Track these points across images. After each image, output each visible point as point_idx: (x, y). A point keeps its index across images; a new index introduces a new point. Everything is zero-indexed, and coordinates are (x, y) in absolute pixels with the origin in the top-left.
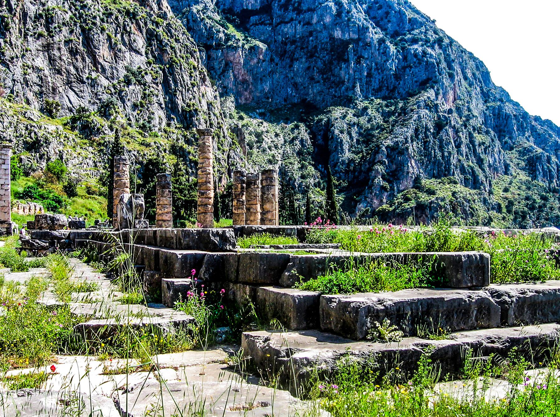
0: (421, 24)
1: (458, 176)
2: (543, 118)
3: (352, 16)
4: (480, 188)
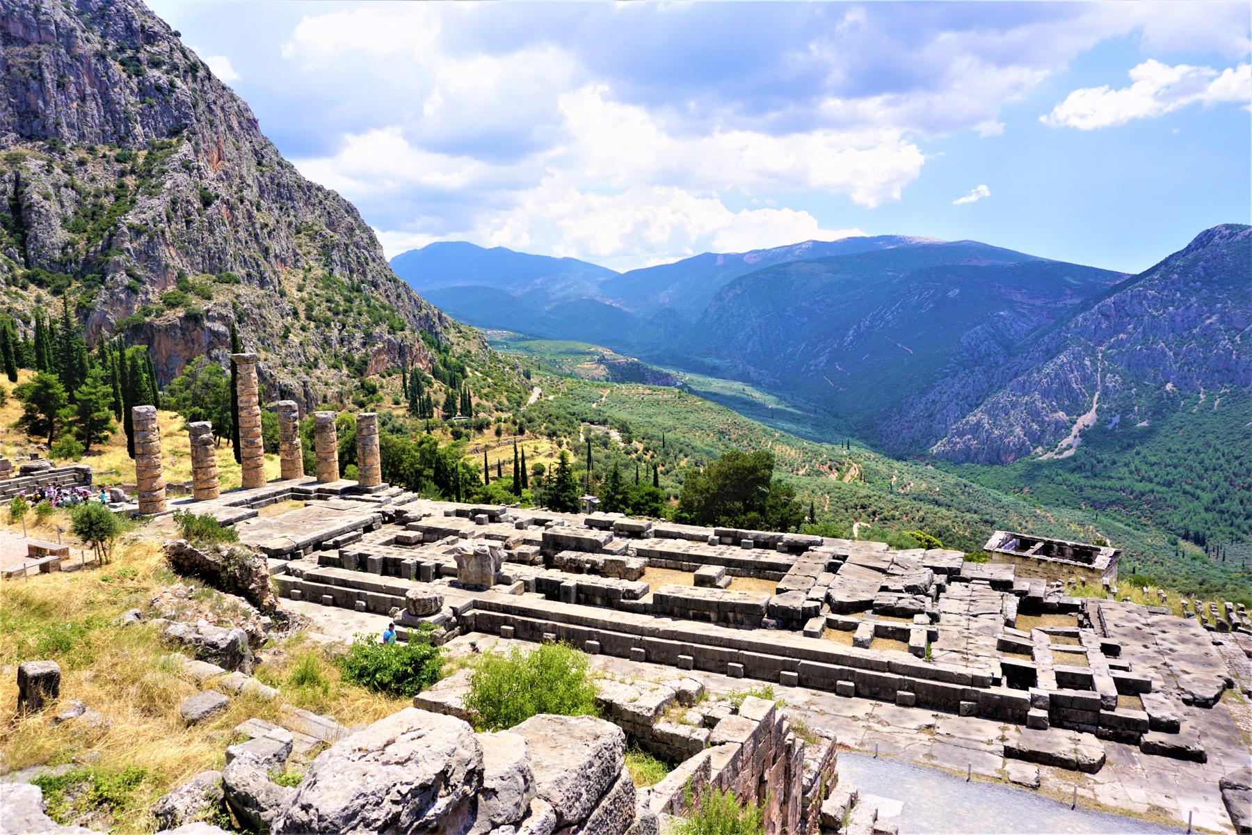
2: (327, 188)
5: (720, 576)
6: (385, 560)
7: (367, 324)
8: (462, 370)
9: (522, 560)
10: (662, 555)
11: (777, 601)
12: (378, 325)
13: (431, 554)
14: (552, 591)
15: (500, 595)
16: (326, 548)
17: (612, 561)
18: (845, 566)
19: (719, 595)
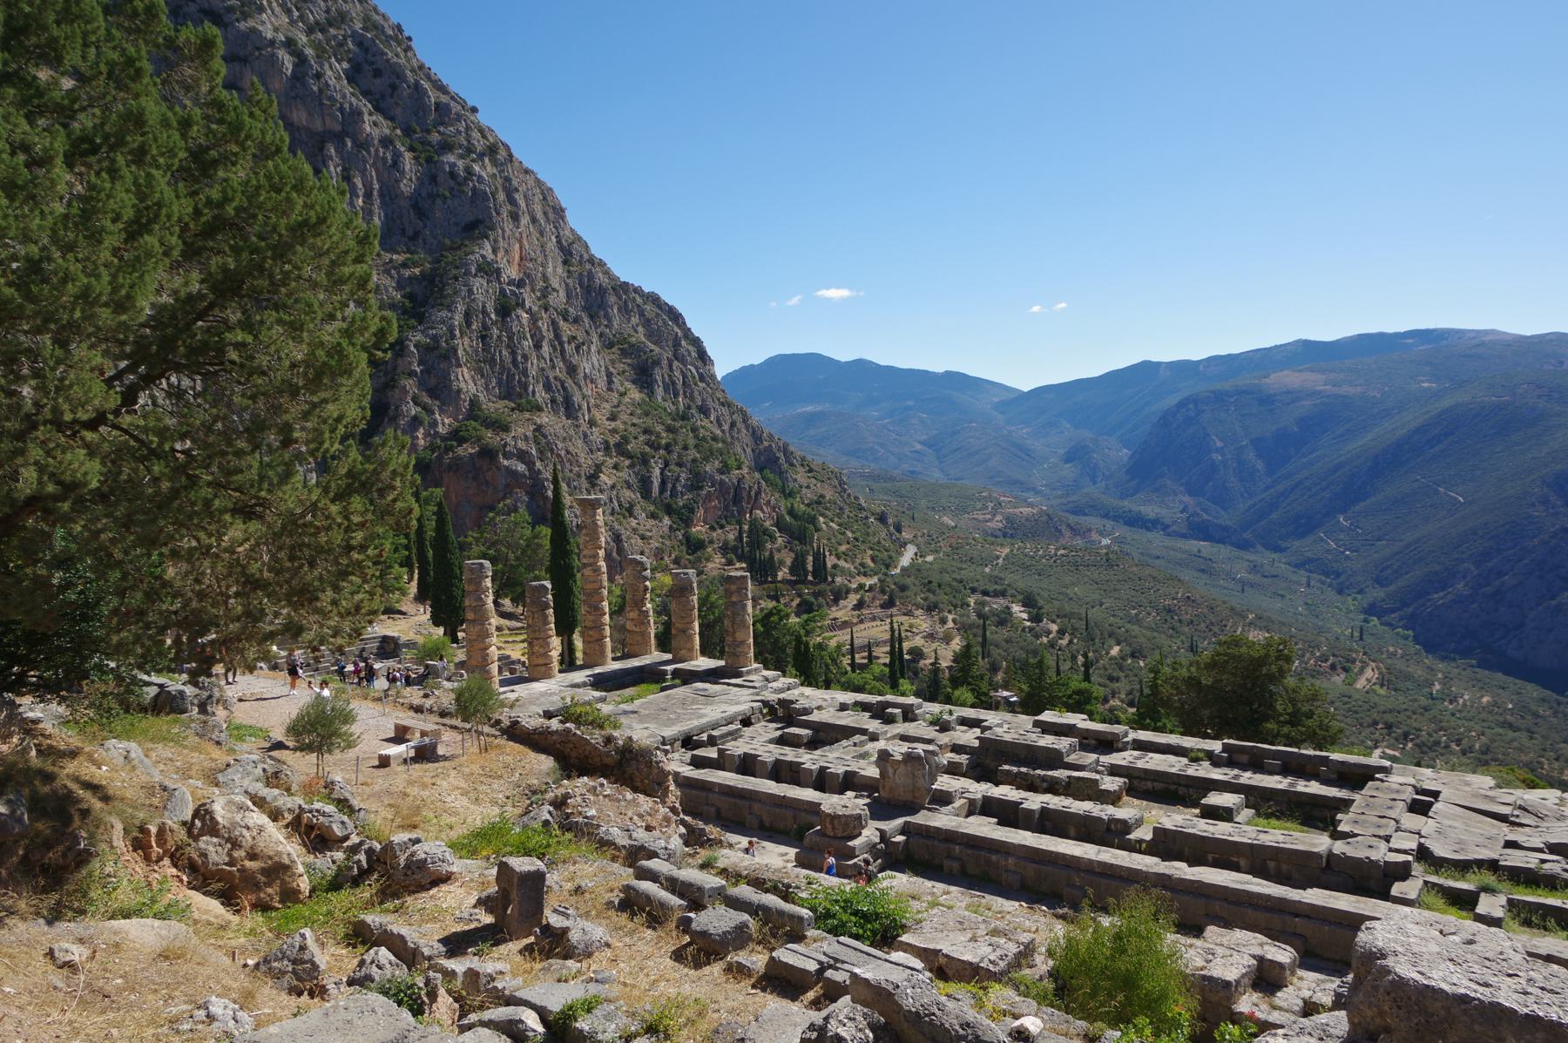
0: (459, 117)
1: (541, 395)
2: (646, 290)
3: (327, 85)
4: (577, 418)
6: (777, 761)
7: (694, 461)
8: (813, 520)
9: (953, 770)
11: (1339, 847)
12: (706, 459)
13: (836, 758)
14: (1008, 814)
15: (942, 819)
16: (700, 745)
17: (1079, 779)
18: (1437, 806)
19: (1254, 835)
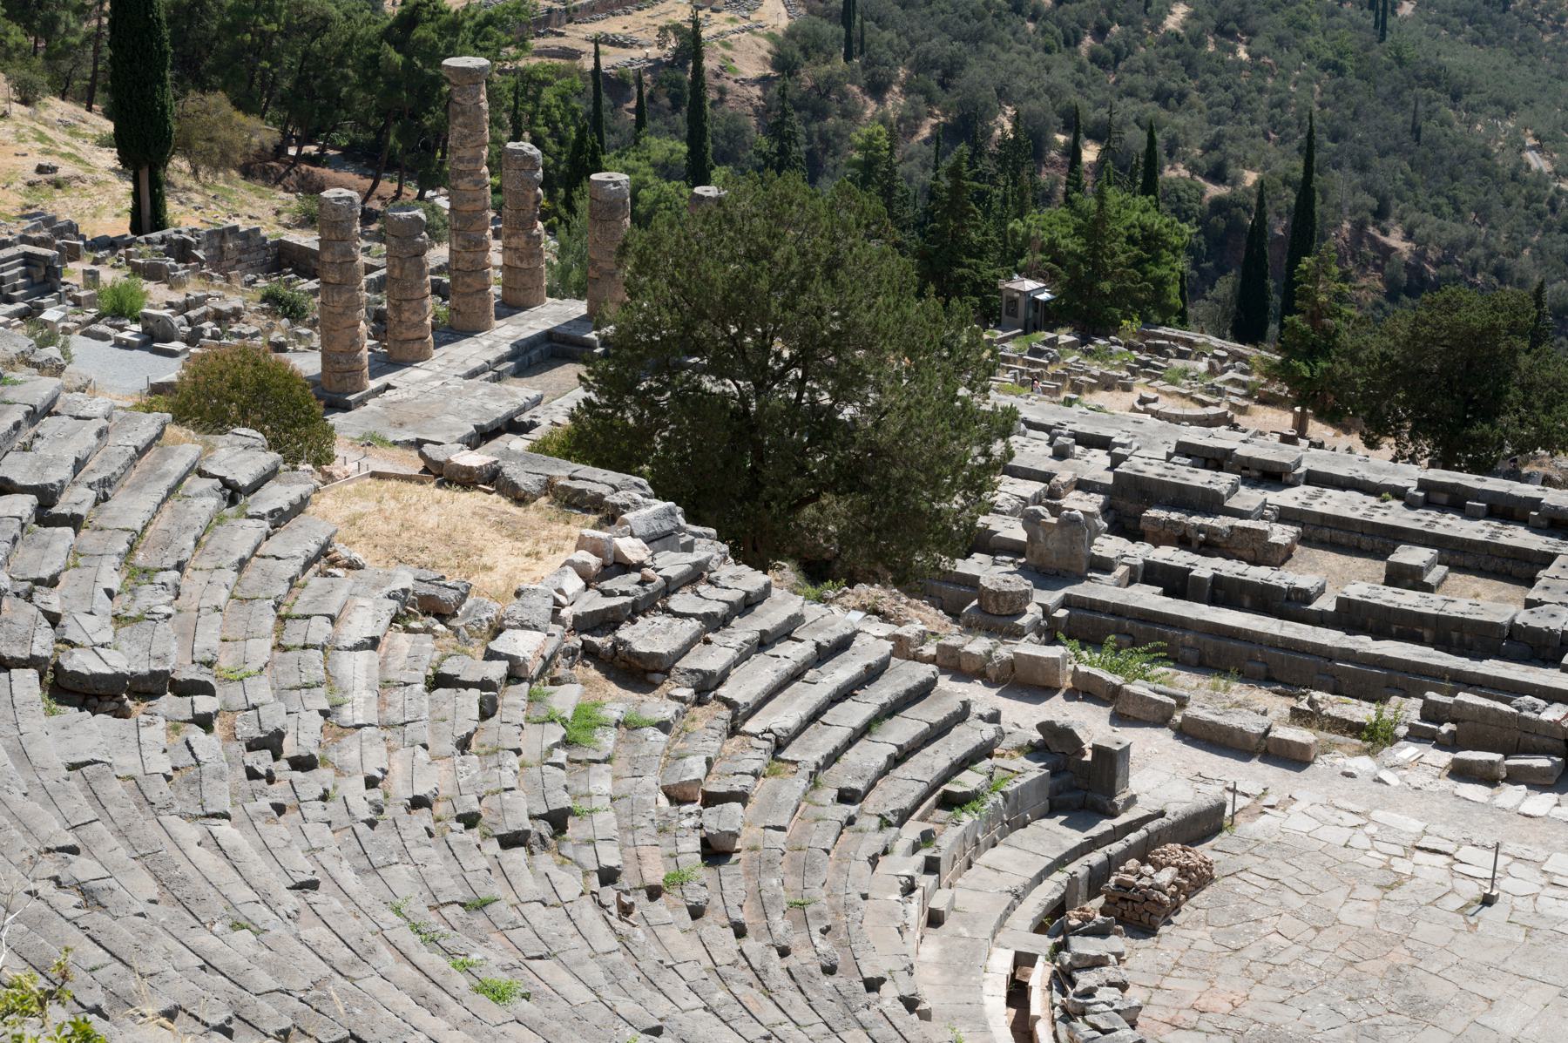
5: (1430, 566)
10: (1326, 520)
11: (1524, 618)
14: (1176, 583)
15: (1103, 589)
17: (1244, 530)
19: (1440, 605)
